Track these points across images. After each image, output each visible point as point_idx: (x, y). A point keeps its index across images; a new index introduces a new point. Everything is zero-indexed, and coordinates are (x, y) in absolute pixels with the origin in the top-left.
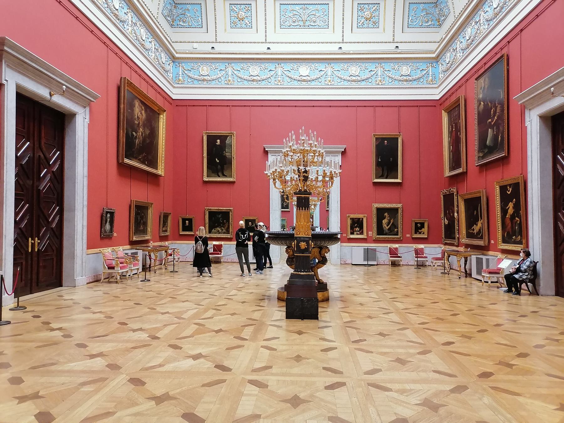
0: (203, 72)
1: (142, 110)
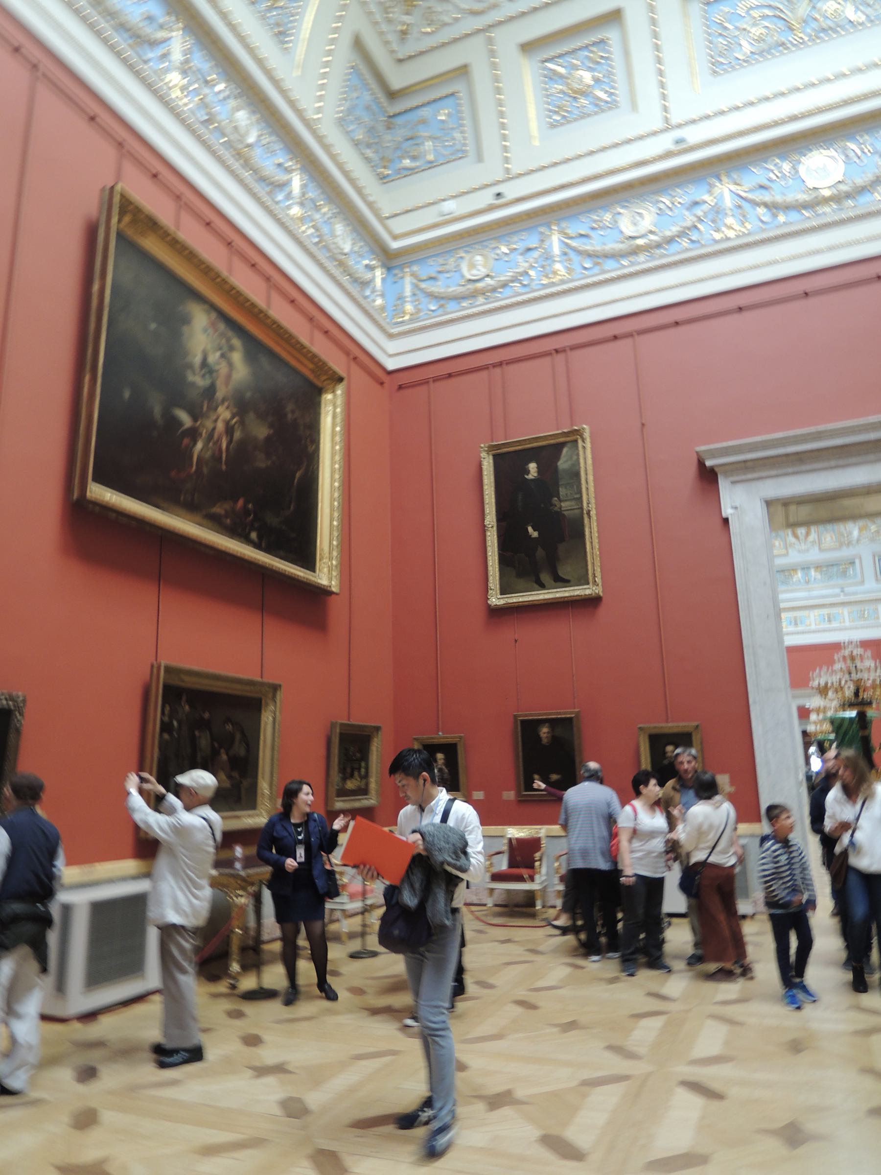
0: (474, 272)
1: (232, 348)
